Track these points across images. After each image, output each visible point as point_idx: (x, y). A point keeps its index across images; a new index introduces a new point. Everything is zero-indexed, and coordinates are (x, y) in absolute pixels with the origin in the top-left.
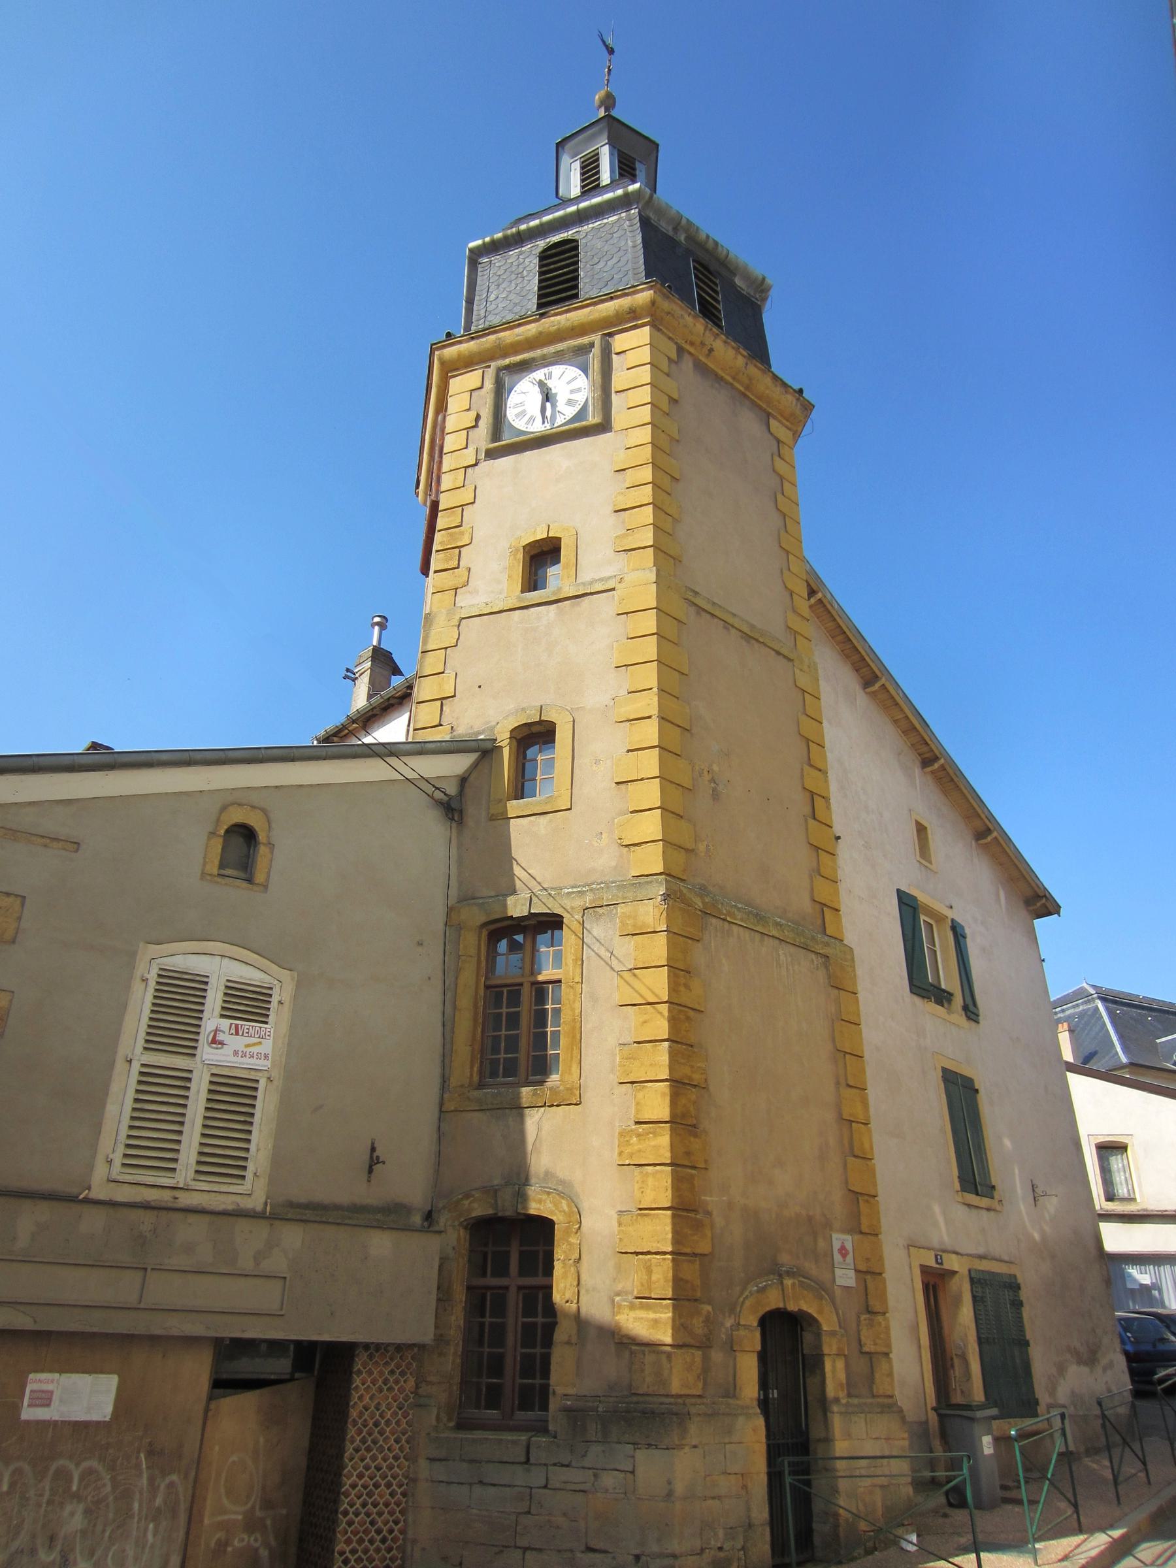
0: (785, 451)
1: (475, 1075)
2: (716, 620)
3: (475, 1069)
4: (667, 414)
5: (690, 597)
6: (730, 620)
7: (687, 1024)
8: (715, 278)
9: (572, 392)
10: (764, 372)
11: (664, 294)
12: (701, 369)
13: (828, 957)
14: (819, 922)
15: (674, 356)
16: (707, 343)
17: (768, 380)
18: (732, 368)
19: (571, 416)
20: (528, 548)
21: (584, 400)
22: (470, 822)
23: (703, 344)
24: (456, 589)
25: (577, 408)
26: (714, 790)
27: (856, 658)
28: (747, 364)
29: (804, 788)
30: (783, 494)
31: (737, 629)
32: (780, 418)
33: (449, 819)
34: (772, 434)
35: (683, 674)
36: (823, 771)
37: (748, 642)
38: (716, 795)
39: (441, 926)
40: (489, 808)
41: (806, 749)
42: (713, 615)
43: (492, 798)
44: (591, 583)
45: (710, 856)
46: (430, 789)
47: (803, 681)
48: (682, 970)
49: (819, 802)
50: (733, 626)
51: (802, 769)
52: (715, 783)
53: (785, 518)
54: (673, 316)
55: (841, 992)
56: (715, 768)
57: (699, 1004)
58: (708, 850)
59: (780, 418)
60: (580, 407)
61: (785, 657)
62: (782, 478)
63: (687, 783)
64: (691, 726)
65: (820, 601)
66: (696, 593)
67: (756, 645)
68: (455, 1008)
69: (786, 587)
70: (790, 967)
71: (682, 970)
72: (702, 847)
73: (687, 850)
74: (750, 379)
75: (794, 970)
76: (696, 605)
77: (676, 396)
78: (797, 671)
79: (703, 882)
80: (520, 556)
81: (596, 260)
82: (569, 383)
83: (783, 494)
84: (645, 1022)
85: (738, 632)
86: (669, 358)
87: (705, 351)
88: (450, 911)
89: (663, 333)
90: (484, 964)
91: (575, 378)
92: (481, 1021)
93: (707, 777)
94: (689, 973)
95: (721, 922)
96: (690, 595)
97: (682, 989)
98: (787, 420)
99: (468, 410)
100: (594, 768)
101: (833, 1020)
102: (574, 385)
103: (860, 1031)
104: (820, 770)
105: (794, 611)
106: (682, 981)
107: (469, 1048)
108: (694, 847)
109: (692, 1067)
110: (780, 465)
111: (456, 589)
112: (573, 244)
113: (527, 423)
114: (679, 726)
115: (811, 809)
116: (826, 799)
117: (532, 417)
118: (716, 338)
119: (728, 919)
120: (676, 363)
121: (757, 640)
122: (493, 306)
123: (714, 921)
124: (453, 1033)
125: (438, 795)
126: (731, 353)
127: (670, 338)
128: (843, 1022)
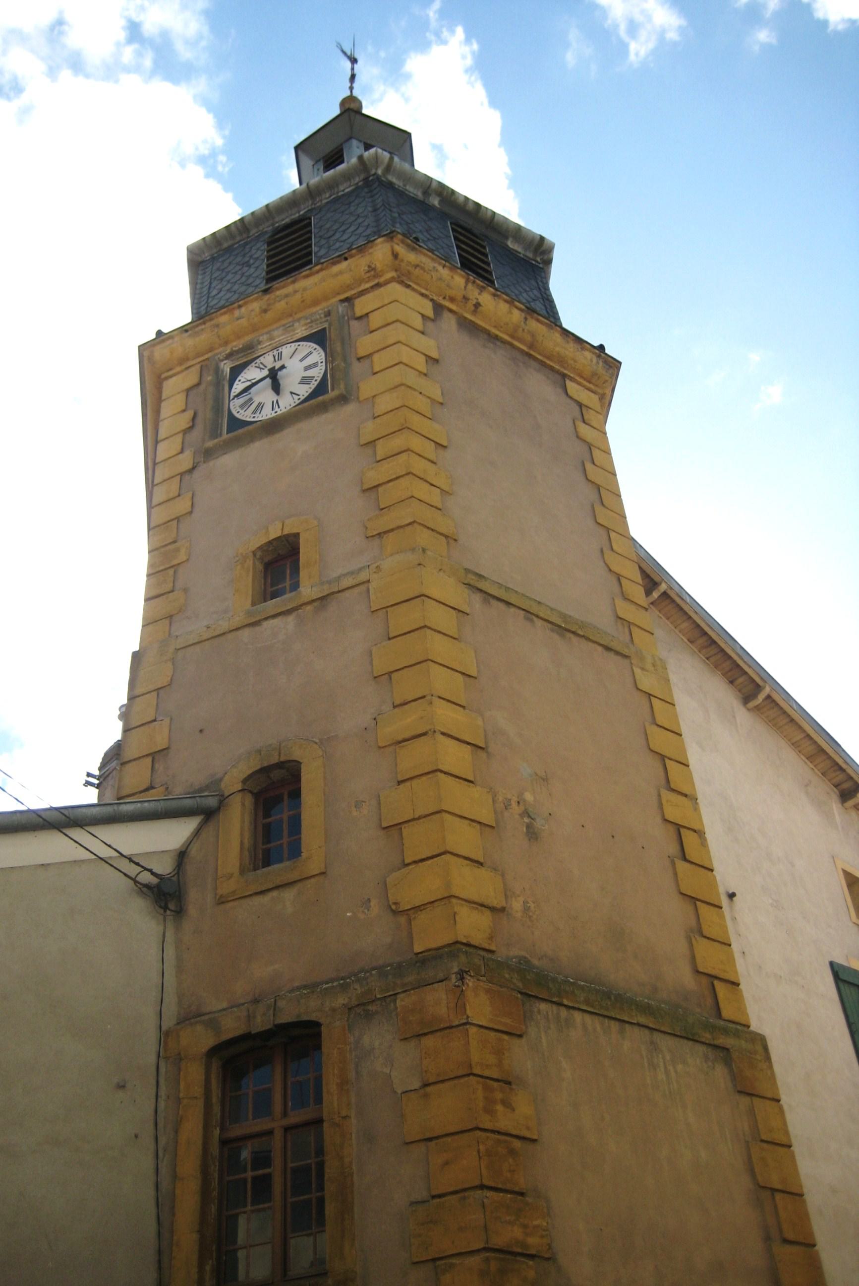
0: (590, 415)
1: (207, 1276)
2: (512, 610)
3: (208, 1268)
4: (425, 375)
5: (472, 582)
6: (535, 609)
7: (511, 1160)
8: (482, 240)
9: (307, 368)
10: (549, 327)
11: (408, 246)
12: (469, 327)
13: (728, 1050)
14: (709, 1001)
15: (430, 312)
16: (471, 297)
17: (557, 336)
18: (507, 324)
19: (306, 395)
20: (259, 554)
21: (321, 375)
22: (192, 911)
23: (466, 298)
24: (171, 617)
25: (314, 385)
26: (529, 826)
27: (727, 665)
28: (526, 319)
29: (666, 820)
30: (593, 463)
31: (542, 619)
32: (578, 378)
33: (161, 907)
34: (571, 398)
35: (469, 676)
36: (692, 798)
37: (562, 636)
38: (532, 834)
39: (152, 1059)
40: (216, 889)
41: (661, 769)
42: (508, 604)
43: (219, 873)
44: (339, 578)
45: (530, 917)
46: (133, 870)
47: (647, 682)
48: (497, 1080)
49: (689, 838)
50: (537, 616)
51: (659, 796)
52: (529, 816)
53: (599, 490)
54: (423, 269)
55: (755, 1099)
56: (529, 797)
57: (528, 1128)
58: (526, 909)
59: (578, 378)
60: (316, 383)
61: (617, 653)
62: (590, 446)
63: (486, 815)
64: (486, 742)
65: (665, 594)
66: (481, 577)
67: (574, 639)
68: (175, 1177)
69: (610, 570)
70: (671, 1068)
71: (497, 1080)
72: (517, 905)
73: (493, 909)
74: (533, 336)
75: (676, 1072)
76: (481, 591)
77: (434, 354)
78: (637, 671)
79: (523, 953)
80: (250, 563)
81: (331, 233)
82: (301, 360)
83: (593, 463)
84: (447, 1163)
85: (545, 624)
86: (423, 316)
87: (470, 305)
88: (165, 1036)
89: (414, 290)
90: (217, 1109)
91: (310, 353)
92: (215, 1193)
93: (516, 809)
94: (509, 1083)
95: (555, 1007)
96: (472, 579)
97: (499, 1108)
98: (590, 382)
99: (184, 411)
100: (355, 813)
101: (747, 1142)
102: (309, 361)
103: (792, 1156)
104: (686, 796)
105: (626, 599)
106: (499, 1096)
107: (195, 1236)
108: (504, 904)
109: (525, 1226)
110: (583, 429)
111: (171, 617)
112: (306, 222)
113: (254, 412)
114: (468, 743)
115: (678, 847)
116: (700, 833)
117: (260, 404)
118: (481, 291)
119: (566, 1002)
120: (433, 320)
121: (574, 633)
122: (215, 302)
123: (543, 1006)
124: (174, 1214)
125: (146, 877)
126: (503, 307)
127: (422, 295)
128: (765, 1145)
